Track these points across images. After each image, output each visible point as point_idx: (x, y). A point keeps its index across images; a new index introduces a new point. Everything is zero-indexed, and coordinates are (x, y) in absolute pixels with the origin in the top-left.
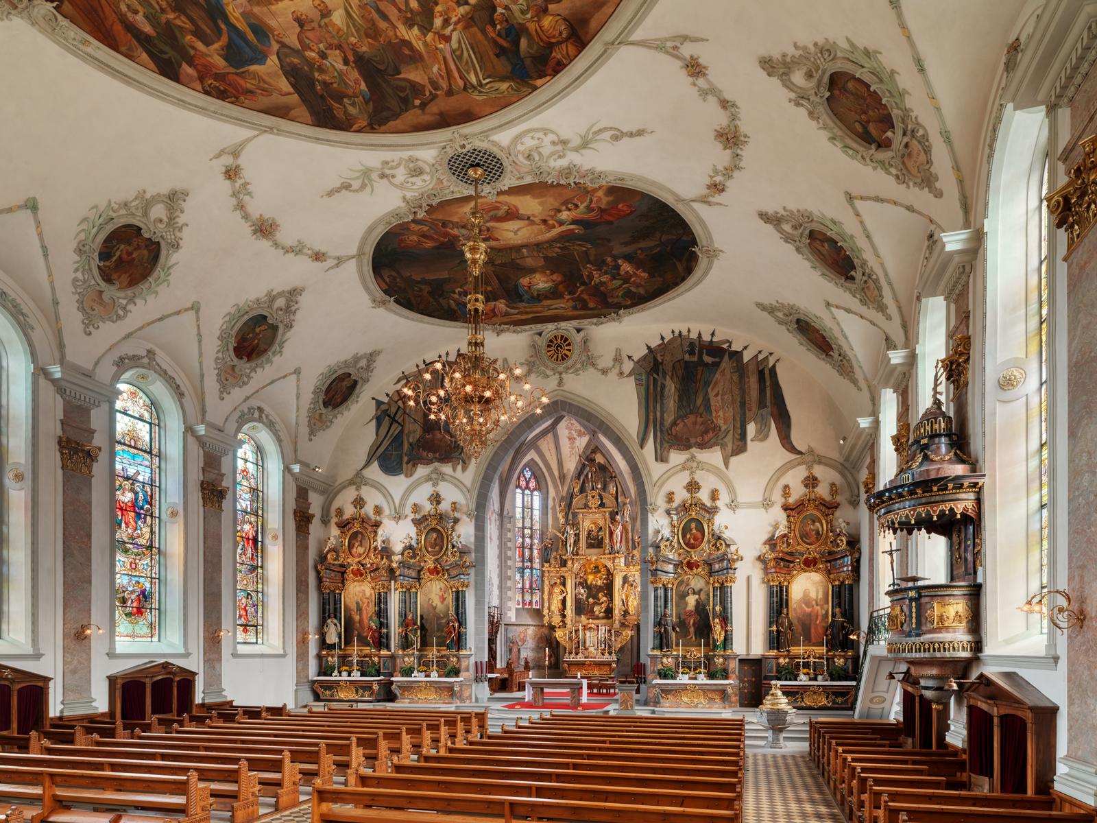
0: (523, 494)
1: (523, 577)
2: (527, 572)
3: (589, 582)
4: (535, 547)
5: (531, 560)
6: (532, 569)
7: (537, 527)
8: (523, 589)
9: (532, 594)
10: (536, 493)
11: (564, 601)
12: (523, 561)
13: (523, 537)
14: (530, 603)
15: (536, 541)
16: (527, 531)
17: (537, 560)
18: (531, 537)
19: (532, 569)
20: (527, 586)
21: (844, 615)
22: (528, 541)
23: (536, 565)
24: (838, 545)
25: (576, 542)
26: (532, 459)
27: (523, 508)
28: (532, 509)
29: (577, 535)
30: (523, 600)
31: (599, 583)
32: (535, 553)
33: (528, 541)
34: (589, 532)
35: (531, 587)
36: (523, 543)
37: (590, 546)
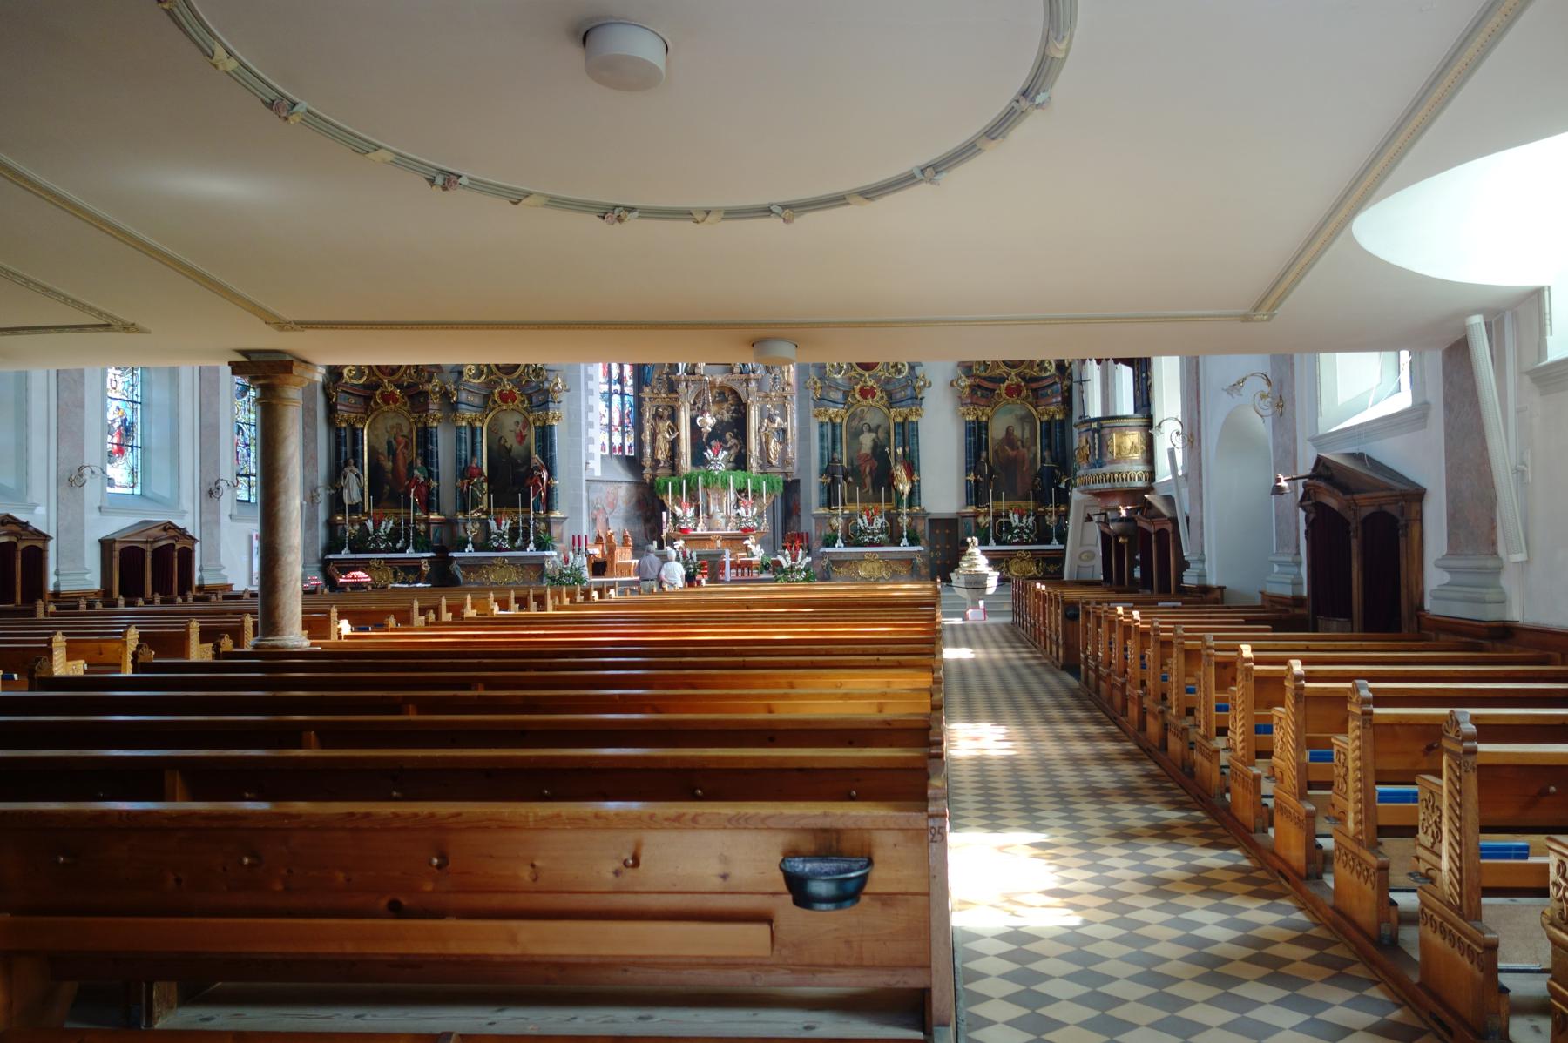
1: (610, 407)
2: (616, 399)
5: (621, 380)
6: (622, 394)
8: (610, 424)
9: (623, 433)
11: (674, 445)
12: (610, 382)
14: (622, 448)
17: (630, 382)
19: (622, 394)
20: (616, 421)
21: (1054, 460)
23: (629, 390)
24: (1046, 370)
30: (611, 443)
35: (622, 423)
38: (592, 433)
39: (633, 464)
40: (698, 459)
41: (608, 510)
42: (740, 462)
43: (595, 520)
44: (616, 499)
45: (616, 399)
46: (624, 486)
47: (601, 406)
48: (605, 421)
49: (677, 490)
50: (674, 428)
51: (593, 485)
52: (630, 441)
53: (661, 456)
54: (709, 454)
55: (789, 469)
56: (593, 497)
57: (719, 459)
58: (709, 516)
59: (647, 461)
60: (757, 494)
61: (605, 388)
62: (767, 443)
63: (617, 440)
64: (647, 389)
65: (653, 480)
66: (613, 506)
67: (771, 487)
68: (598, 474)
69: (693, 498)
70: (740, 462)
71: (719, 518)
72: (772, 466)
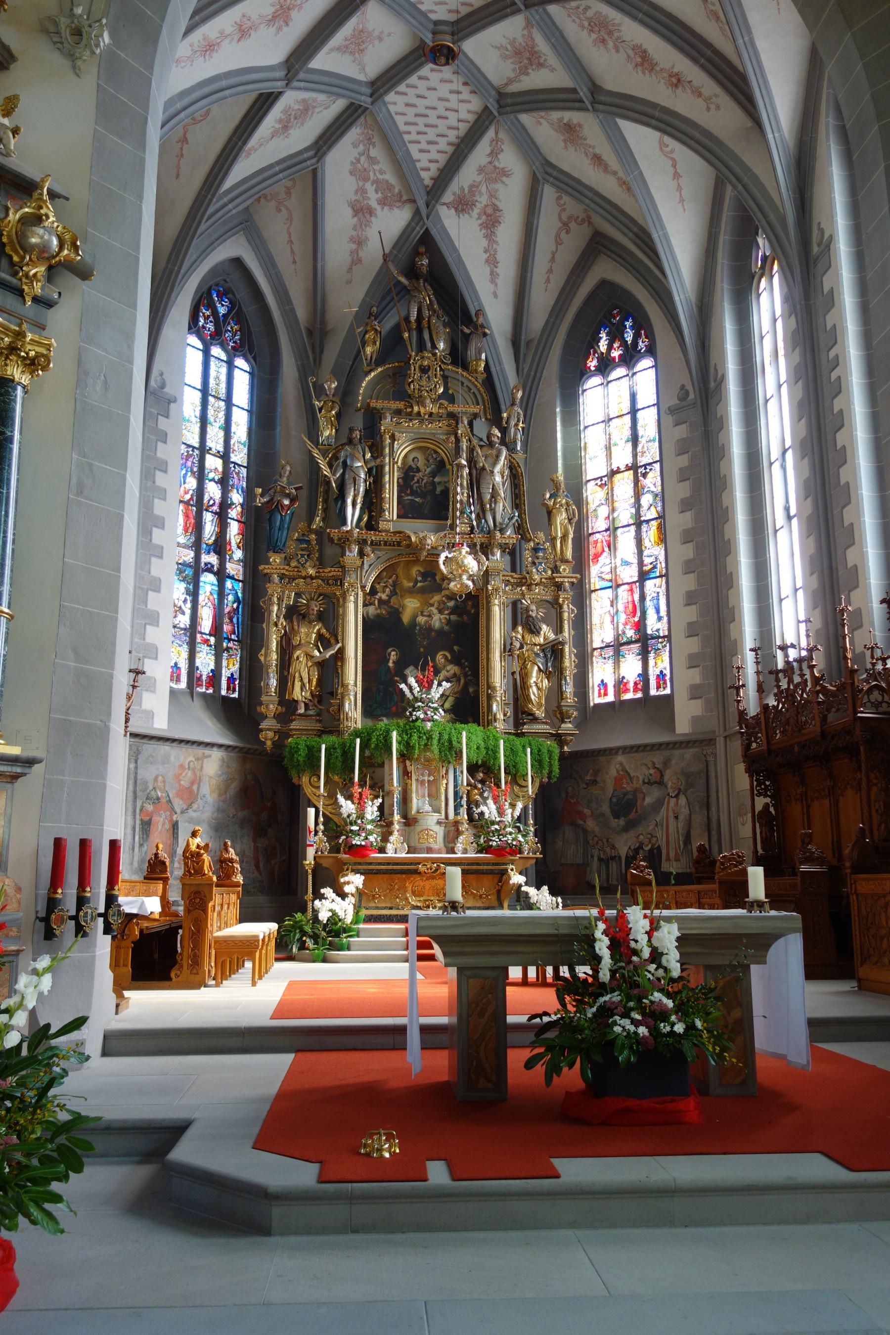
0: (206, 353)
1: (194, 594)
2: (208, 581)
3: (406, 618)
4: (234, 513)
5: (220, 547)
6: (221, 575)
7: (240, 456)
8: (193, 628)
10: (240, 362)
11: (330, 670)
12: (197, 546)
13: (201, 476)
14: (214, 678)
15: (237, 497)
16: (213, 463)
17: (238, 554)
18: (224, 482)
20: (206, 624)
22: (213, 491)
23: (234, 568)
25: (372, 503)
26: (238, 262)
27: (205, 391)
28: (229, 401)
29: (376, 475)
31: (437, 620)
32: (234, 529)
33: (213, 491)
34: (408, 473)
35: (216, 630)
36: (200, 491)
37: (407, 511)
38: (153, 634)
39: (237, 711)
40: (382, 697)
41: (178, 804)
42: (468, 707)
43: (146, 826)
44: (197, 780)
45: (208, 581)
46: (217, 755)
47: (179, 590)
48: (184, 620)
49: (341, 763)
50: (331, 634)
51: (149, 748)
52: (231, 667)
53: (298, 693)
54: (411, 686)
55: (567, 727)
56: (147, 773)
57: (430, 695)
58: (409, 821)
59: (270, 704)
60: (515, 775)
61: (188, 556)
62: (525, 676)
63: (205, 661)
64: (276, 559)
65: (279, 745)
66: (190, 796)
67: (538, 762)
68: (161, 724)
69: (378, 787)
70: (468, 707)
71: (432, 824)
72: (535, 719)
